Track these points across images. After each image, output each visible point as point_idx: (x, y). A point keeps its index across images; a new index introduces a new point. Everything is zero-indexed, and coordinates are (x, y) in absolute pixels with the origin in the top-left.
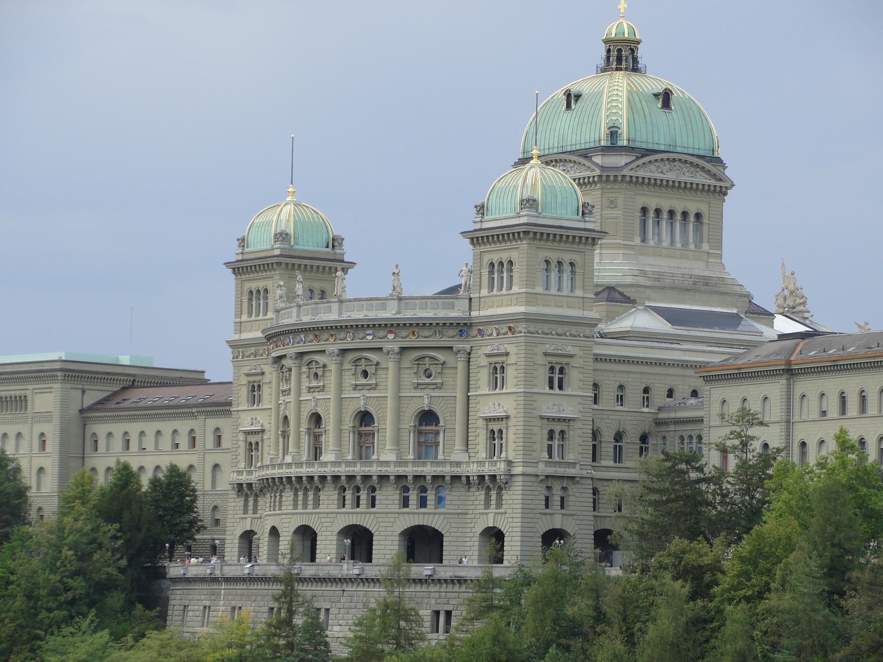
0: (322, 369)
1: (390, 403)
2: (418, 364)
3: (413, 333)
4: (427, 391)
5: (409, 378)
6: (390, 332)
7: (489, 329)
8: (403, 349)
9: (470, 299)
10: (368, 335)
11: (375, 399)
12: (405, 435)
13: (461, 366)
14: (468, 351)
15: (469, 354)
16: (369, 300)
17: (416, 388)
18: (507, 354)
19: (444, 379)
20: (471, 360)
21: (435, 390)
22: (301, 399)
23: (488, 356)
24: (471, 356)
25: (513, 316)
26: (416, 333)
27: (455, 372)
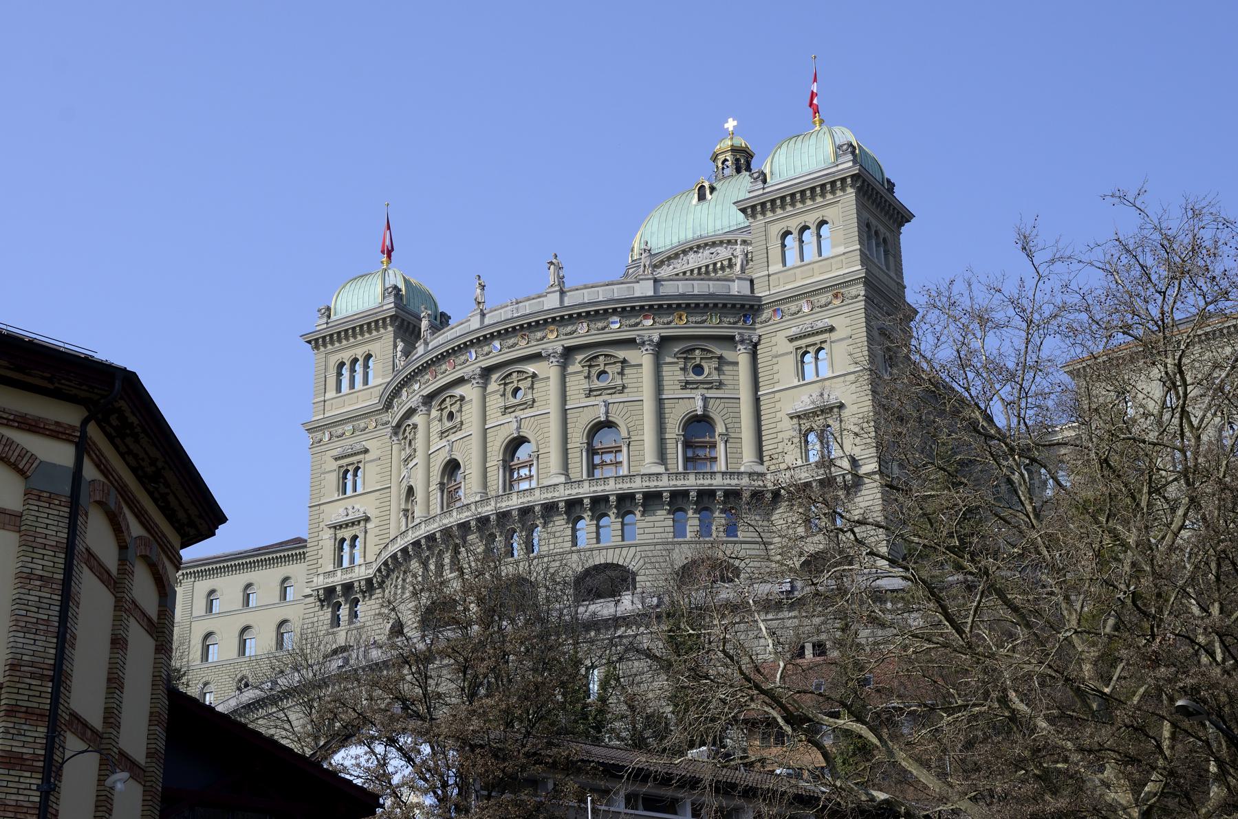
0: (530, 379)
1: (648, 407)
2: (685, 358)
3: (680, 318)
4: (699, 392)
5: (673, 374)
6: (646, 317)
7: (793, 307)
8: (664, 340)
9: (752, 281)
10: (613, 323)
11: (622, 404)
12: (670, 446)
13: (743, 358)
14: (755, 339)
15: (755, 345)
16: (607, 285)
17: (684, 388)
18: (832, 329)
19: (722, 377)
20: (758, 352)
21: (709, 391)
22: (486, 427)
23: (791, 340)
24: (758, 347)
25: (844, 278)
26: (684, 317)
27: (735, 368)
